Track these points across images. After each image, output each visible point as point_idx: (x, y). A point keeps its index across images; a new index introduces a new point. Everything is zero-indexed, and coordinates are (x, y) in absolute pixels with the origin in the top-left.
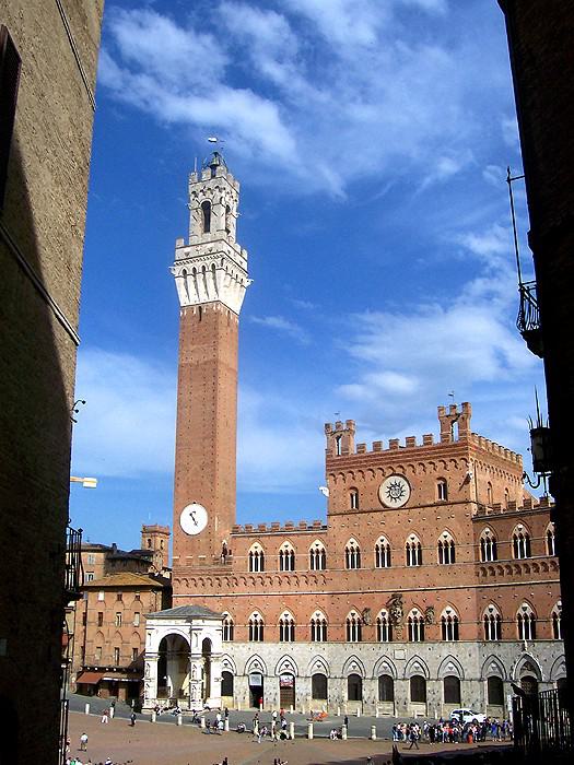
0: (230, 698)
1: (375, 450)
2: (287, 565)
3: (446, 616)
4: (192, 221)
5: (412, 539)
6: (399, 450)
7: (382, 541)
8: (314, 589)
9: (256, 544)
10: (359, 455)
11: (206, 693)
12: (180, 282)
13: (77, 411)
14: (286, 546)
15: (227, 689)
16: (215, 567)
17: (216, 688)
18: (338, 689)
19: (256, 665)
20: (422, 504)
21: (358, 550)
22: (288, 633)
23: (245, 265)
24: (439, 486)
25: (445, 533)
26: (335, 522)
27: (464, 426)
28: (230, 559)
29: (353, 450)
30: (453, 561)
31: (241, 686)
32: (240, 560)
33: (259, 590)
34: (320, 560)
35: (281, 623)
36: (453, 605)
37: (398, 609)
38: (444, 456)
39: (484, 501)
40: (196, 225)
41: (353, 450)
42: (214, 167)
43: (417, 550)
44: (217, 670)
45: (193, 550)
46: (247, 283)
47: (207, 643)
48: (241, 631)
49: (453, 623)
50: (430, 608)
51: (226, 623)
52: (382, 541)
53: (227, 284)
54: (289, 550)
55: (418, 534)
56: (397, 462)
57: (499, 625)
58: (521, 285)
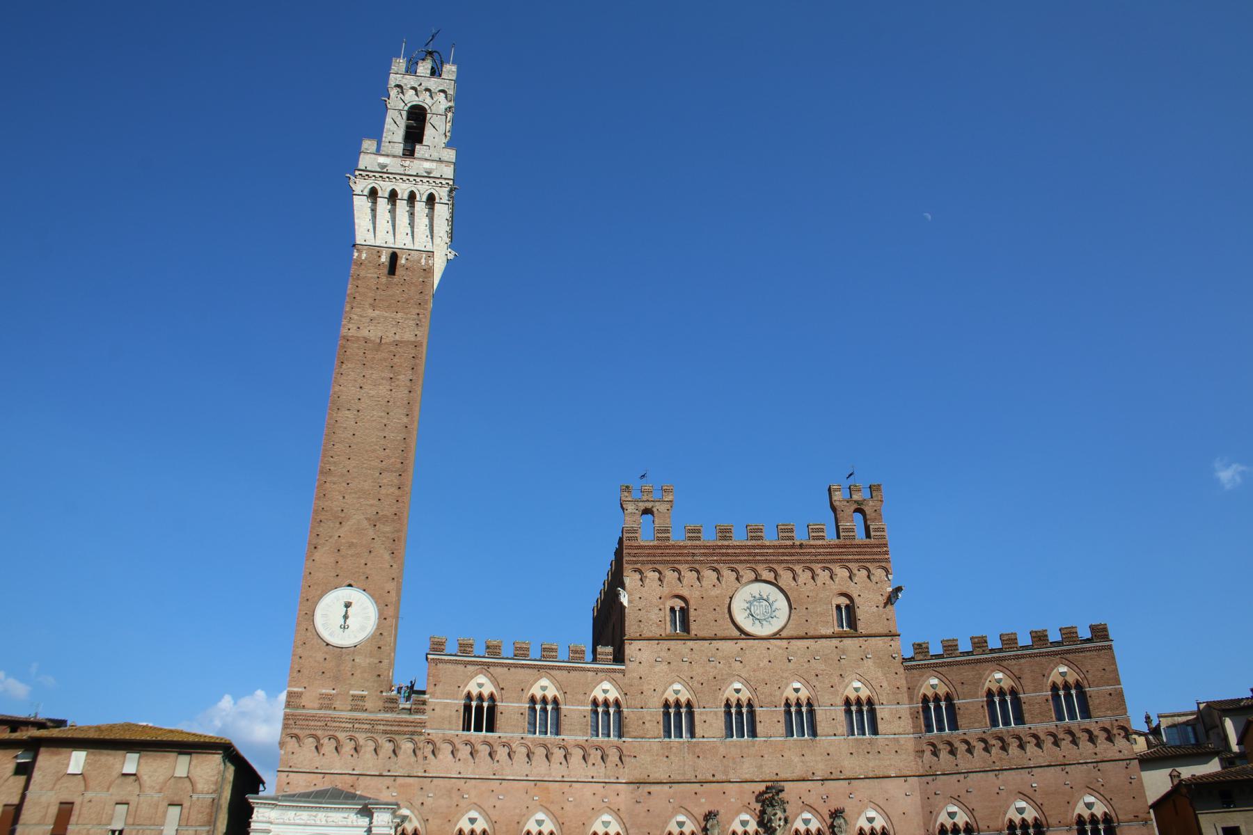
5: (795, 689)
7: (738, 691)
8: (599, 771)
9: (481, 679)
10: (689, 543)
12: (361, 205)
14: (544, 687)
16: (389, 716)
20: (811, 633)
24: (838, 607)
25: (857, 684)
28: (424, 703)
30: (875, 731)
33: (484, 766)
37: (780, 814)
38: (849, 561)
40: (395, 129)
45: (336, 679)
50: (837, 814)
52: (737, 690)
54: (550, 696)
55: (807, 682)
56: (766, 561)
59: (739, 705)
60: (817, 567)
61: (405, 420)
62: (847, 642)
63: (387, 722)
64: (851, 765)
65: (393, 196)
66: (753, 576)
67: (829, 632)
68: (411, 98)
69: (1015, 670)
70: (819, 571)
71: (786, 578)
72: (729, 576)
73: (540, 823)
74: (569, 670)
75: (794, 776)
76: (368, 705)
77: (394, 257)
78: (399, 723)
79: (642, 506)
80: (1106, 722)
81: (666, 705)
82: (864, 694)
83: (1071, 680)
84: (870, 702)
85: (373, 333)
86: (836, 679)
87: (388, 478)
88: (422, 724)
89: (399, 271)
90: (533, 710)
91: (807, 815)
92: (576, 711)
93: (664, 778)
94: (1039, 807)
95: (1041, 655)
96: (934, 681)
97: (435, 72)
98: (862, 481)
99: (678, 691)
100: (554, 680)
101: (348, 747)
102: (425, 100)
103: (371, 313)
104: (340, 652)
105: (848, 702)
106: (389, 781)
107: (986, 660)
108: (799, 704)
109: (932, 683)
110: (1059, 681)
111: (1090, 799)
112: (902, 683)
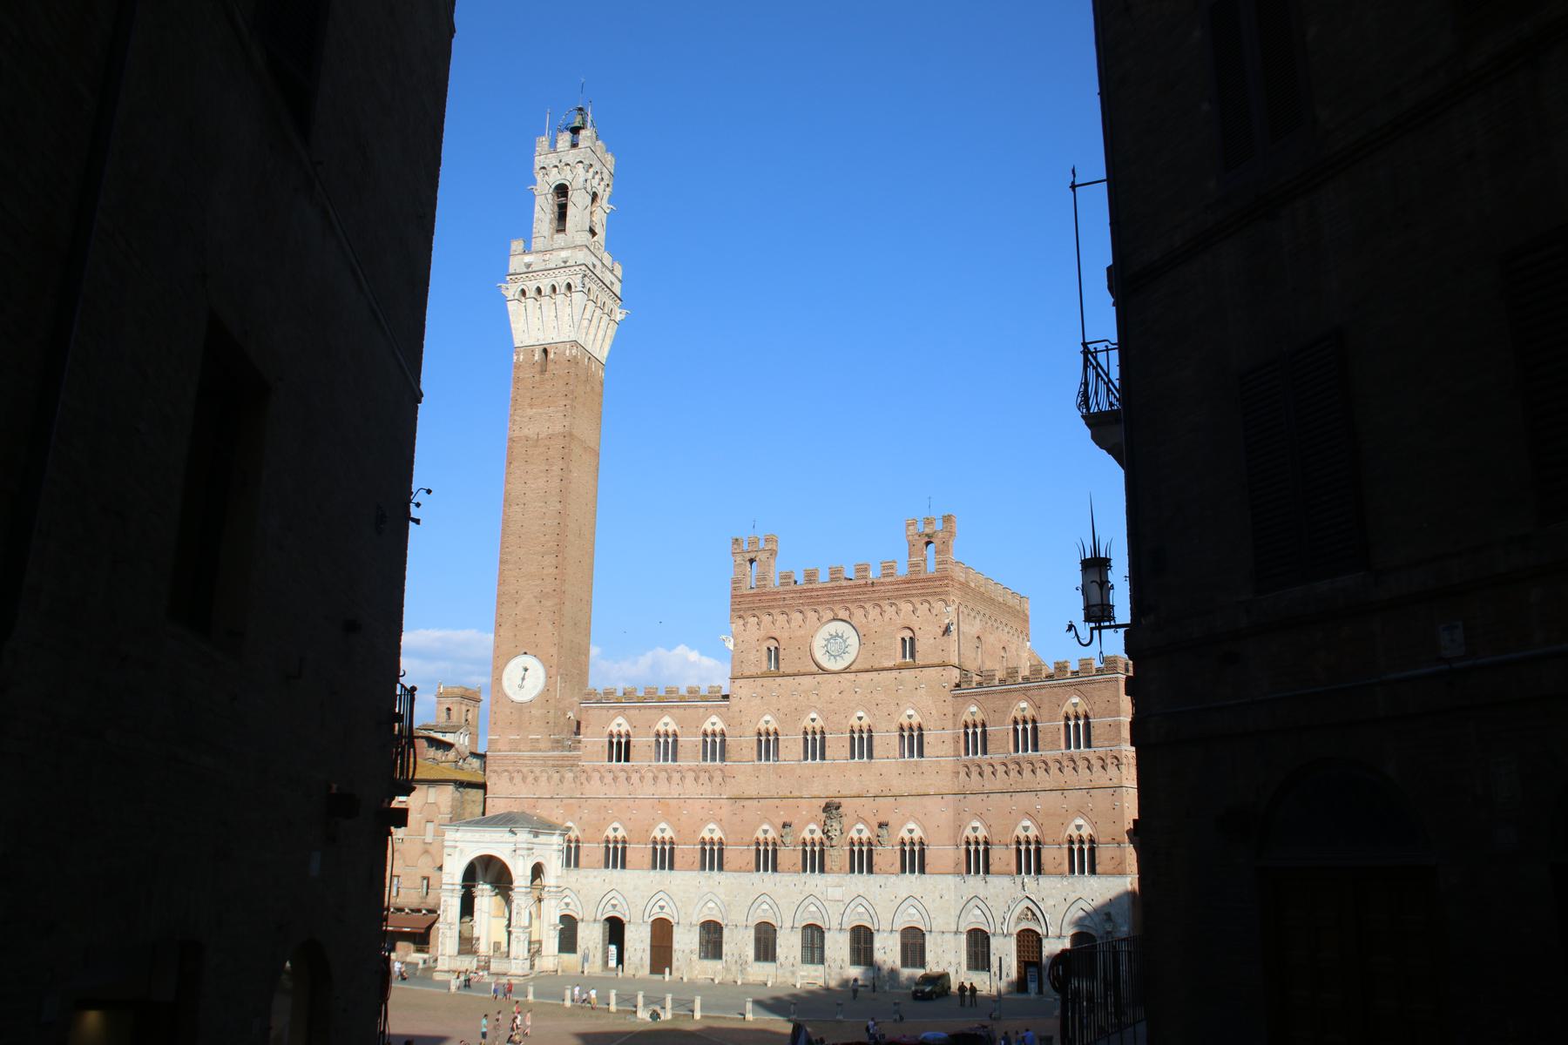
0: (572, 956)
1: (810, 581)
2: (666, 754)
3: (907, 838)
4: (538, 213)
5: (860, 717)
6: (844, 583)
8: (706, 790)
9: (620, 720)
11: (535, 950)
13: (418, 505)
14: (666, 723)
15: (568, 937)
17: (551, 943)
18: (739, 943)
19: (614, 906)
21: (776, 733)
22: (664, 857)
23: (617, 288)
26: (744, 690)
27: (944, 549)
29: (774, 582)
30: (921, 754)
31: (591, 935)
32: (594, 742)
33: (622, 790)
34: (716, 747)
35: (655, 842)
36: (917, 821)
39: (971, 666)
41: (774, 582)
42: (575, 131)
43: (865, 736)
44: (552, 913)
46: (619, 316)
47: (537, 871)
48: (592, 851)
49: (916, 848)
51: (569, 841)
52: (813, 719)
53: (588, 315)
55: (868, 711)
56: (843, 601)
57: (986, 851)
58: (1085, 344)
59: (814, 733)
60: (885, 605)
61: (559, 506)
62: (905, 673)
63: (555, 759)
64: (899, 785)
65: (539, 290)
66: (830, 615)
67: (891, 664)
68: (555, 178)
69: (1037, 699)
70: (887, 608)
71: (859, 613)
72: (811, 615)
73: (663, 831)
74: (685, 708)
75: (853, 793)
76: (542, 745)
77: (545, 351)
78: (563, 759)
79: (748, 556)
80: (1101, 751)
81: (760, 734)
82: (915, 722)
83: (1081, 711)
84: (920, 728)
85: (530, 431)
86: (893, 708)
87: (550, 560)
88: (578, 758)
89: (551, 366)
90: (658, 742)
91: (860, 826)
92: (690, 742)
93: (754, 794)
94: (1040, 827)
95: (1060, 686)
96: (974, 709)
97: (574, 145)
98: (937, 514)
99: (769, 721)
100: (672, 717)
101: (530, 779)
102: (565, 177)
103: (530, 412)
104: (521, 707)
105: (902, 729)
106: (558, 802)
107: (1015, 690)
108: (861, 731)
109: (972, 711)
110: (1071, 712)
111: (1080, 821)
112: (949, 710)
